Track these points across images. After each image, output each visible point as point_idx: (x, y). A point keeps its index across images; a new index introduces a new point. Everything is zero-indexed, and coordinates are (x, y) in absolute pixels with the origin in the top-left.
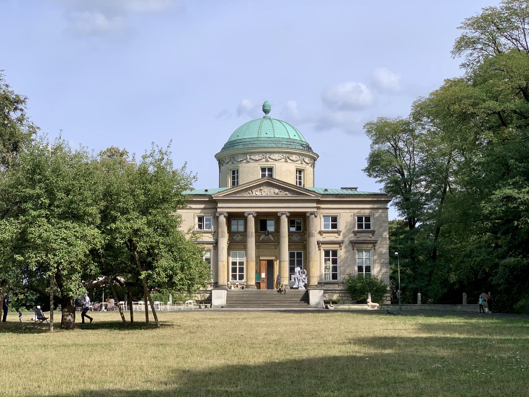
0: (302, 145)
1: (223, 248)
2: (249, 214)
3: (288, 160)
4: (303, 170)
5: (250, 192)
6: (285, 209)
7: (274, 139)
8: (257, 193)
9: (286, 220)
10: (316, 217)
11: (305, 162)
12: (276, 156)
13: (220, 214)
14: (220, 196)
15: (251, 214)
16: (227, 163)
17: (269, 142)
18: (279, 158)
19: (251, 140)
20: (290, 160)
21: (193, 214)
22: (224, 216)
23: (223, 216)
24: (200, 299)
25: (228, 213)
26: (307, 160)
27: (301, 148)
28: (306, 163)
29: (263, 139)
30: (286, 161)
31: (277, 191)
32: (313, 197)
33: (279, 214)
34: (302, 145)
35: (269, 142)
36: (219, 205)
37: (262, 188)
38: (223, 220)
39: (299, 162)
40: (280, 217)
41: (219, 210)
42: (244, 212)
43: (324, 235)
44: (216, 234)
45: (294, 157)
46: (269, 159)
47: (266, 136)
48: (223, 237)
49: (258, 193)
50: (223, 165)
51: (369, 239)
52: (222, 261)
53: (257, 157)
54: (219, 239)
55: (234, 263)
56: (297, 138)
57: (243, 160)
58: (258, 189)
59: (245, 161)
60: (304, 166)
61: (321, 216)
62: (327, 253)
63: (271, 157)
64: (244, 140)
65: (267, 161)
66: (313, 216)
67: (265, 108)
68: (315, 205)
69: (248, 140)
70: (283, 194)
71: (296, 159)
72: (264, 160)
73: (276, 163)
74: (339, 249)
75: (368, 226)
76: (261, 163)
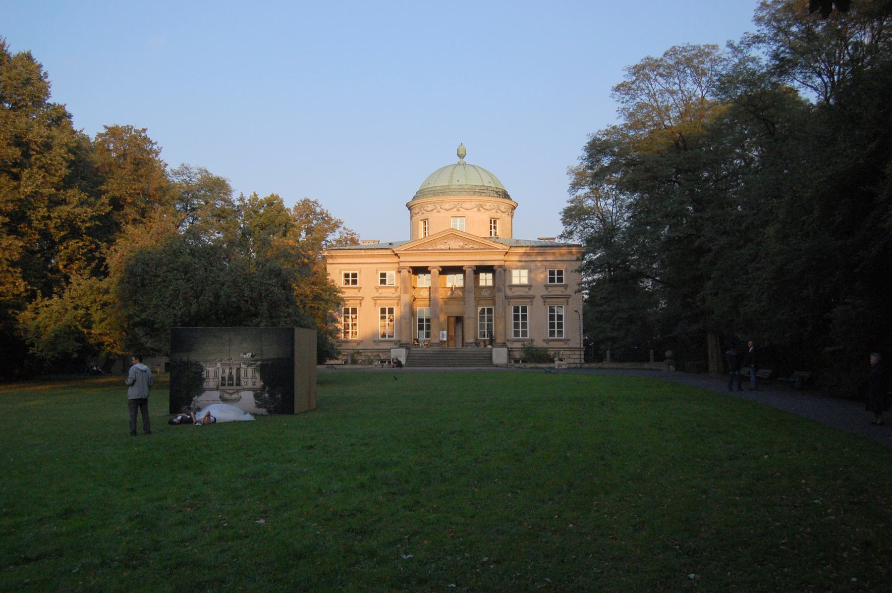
0: (497, 192)
7: (466, 187)
12: (467, 205)
30: (479, 210)
34: (497, 192)
36: (402, 259)
39: (494, 211)
43: (514, 289)
49: (442, 247)
51: (560, 293)
55: (421, 320)
60: (499, 214)
62: (516, 310)
65: (458, 210)
68: (502, 257)
73: (468, 212)
75: (560, 280)
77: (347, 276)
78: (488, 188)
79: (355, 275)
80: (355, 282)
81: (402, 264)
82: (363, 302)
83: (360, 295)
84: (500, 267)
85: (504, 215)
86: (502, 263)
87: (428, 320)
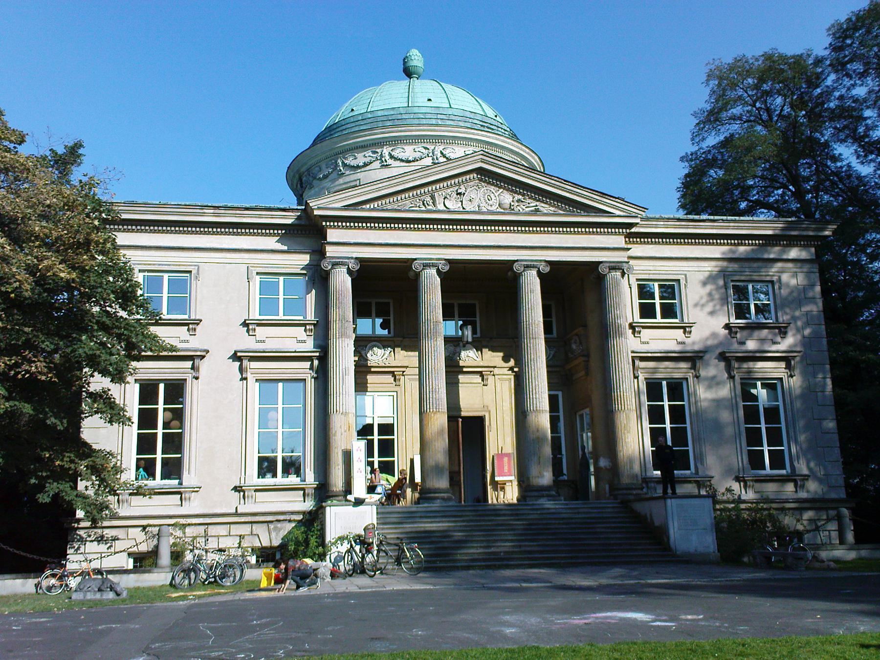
1: (345, 373)
2: (426, 266)
5: (428, 199)
6: (533, 250)
8: (449, 204)
10: (623, 276)
13: (335, 265)
15: (433, 265)
16: (325, 177)
17: (439, 117)
19: (392, 113)
22: (350, 272)
23: (344, 270)
24: (266, 543)
25: (361, 260)
29: (423, 110)
31: (507, 198)
33: (516, 267)
35: (439, 117)
36: (333, 235)
38: (342, 282)
40: (520, 275)
41: (330, 251)
43: (646, 334)
44: (322, 330)
47: (429, 104)
48: (343, 335)
49: (452, 204)
50: (312, 187)
52: (346, 414)
53: (408, 152)
54: (331, 342)
59: (377, 164)
62: (653, 389)
64: (370, 116)
66: (618, 274)
68: (618, 241)
70: (528, 208)
74: (690, 376)
82: (203, 365)
84: (615, 267)
87: (387, 429)
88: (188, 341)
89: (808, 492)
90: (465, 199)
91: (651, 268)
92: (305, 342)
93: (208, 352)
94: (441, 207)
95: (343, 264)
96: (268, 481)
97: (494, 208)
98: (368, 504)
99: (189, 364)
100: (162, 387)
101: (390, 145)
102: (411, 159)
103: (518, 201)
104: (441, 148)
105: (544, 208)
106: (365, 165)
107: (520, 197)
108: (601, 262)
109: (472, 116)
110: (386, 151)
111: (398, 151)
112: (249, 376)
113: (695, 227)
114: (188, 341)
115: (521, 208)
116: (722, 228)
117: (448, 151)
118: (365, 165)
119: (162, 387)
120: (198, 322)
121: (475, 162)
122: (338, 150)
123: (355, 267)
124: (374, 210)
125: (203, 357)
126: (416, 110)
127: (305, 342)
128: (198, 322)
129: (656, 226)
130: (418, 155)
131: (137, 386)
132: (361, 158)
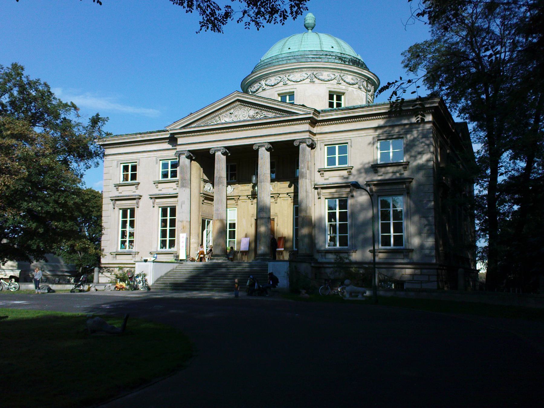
3: (315, 80)
4: (344, 94)
6: (261, 137)
8: (225, 119)
9: (268, 154)
11: (345, 81)
12: (297, 76)
14: (177, 128)
18: (302, 78)
20: (319, 79)
21: (155, 158)
26: (349, 78)
27: (340, 61)
28: (347, 83)
30: (312, 82)
31: (252, 112)
32: (301, 113)
34: (340, 58)
35: (289, 58)
36: (180, 141)
37: (232, 111)
39: (335, 82)
42: (210, 149)
43: (327, 174)
45: (325, 75)
46: (288, 82)
47: (290, 51)
49: (228, 120)
52: (182, 221)
53: (272, 80)
56: (336, 50)
57: (258, 89)
58: (228, 113)
59: (261, 90)
60: (342, 88)
61: (323, 145)
63: (290, 78)
67: (307, 22)
68: (306, 127)
69: (266, 61)
71: (329, 78)
72: (281, 84)
76: (278, 89)
77: (126, 168)
78: (328, 54)
79: (134, 168)
80: (134, 177)
81: (179, 148)
83: (138, 193)
84: (303, 141)
85: (351, 88)
86: (306, 135)
87: (233, 226)
88: (135, 192)
89: (411, 259)
90: (232, 116)
91: (332, 138)
92: (176, 189)
93: (141, 196)
94: (223, 121)
95: (184, 154)
96: (164, 250)
97: (245, 119)
98: (149, 262)
99: (135, 201)
100: (129, 211)
101: (264, 79)
102: (273, 84)
103: (257, 113)
104: (287, 75)
105: (270, 115)
106: (257, 91)
107: (257, 111)
108: (295, 140)
109: (309, 53)
110: (263, 82)
111: (268, 81)
112: (155, 206)
113: (353, 113)
114: (135, 192)
115: (259, 116)
116: (368, 111)
117: (291, 76)
118: (257, 91)
119: (129, 211)
120: (138, 184)
121: (235, 97)
122: (248, 84)
123: (186, 154)
124: (195, 127)
125: (140, 199)
126: (280, 56)
127: (176, 189)
128: (138, 184)
129: (332, 115)
130: (276, 82)
131: (121, 211)
132: (256, 86)
